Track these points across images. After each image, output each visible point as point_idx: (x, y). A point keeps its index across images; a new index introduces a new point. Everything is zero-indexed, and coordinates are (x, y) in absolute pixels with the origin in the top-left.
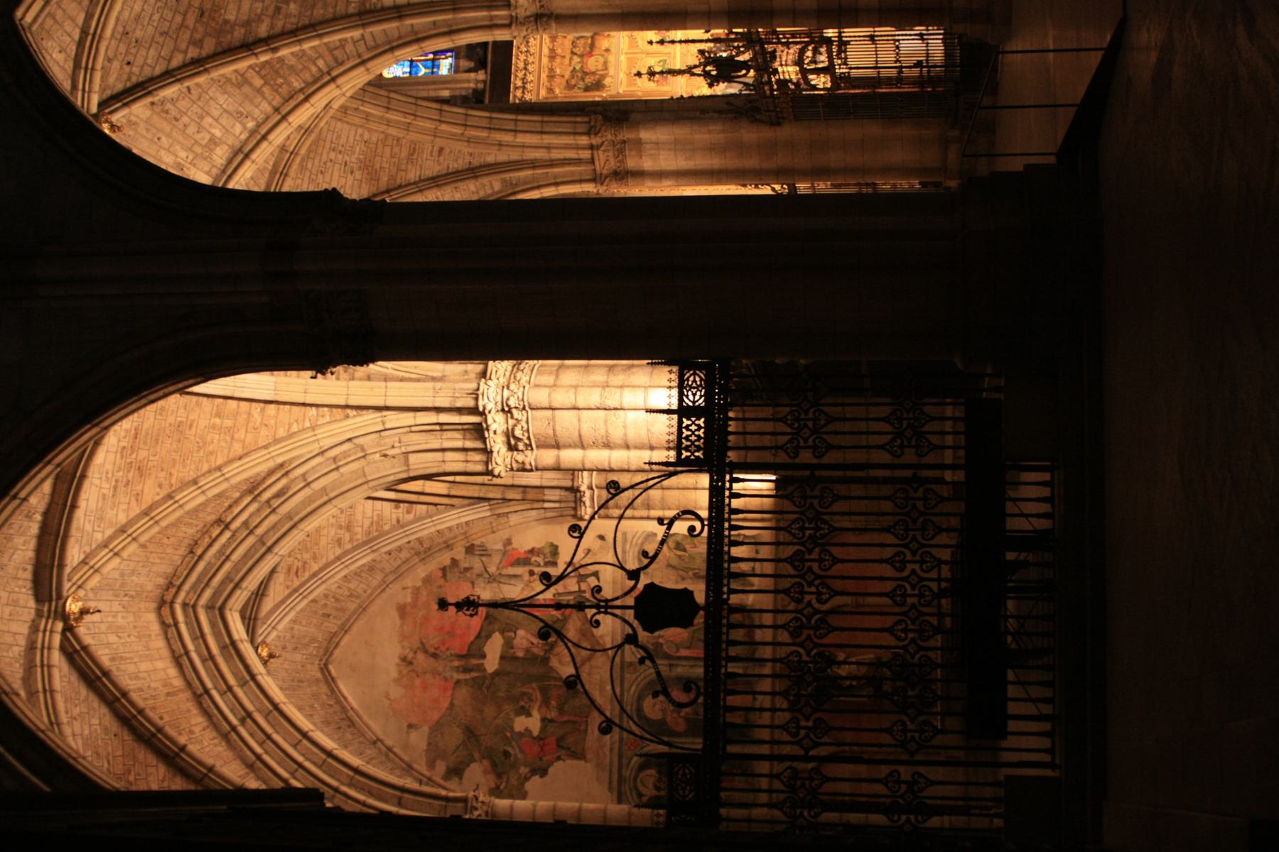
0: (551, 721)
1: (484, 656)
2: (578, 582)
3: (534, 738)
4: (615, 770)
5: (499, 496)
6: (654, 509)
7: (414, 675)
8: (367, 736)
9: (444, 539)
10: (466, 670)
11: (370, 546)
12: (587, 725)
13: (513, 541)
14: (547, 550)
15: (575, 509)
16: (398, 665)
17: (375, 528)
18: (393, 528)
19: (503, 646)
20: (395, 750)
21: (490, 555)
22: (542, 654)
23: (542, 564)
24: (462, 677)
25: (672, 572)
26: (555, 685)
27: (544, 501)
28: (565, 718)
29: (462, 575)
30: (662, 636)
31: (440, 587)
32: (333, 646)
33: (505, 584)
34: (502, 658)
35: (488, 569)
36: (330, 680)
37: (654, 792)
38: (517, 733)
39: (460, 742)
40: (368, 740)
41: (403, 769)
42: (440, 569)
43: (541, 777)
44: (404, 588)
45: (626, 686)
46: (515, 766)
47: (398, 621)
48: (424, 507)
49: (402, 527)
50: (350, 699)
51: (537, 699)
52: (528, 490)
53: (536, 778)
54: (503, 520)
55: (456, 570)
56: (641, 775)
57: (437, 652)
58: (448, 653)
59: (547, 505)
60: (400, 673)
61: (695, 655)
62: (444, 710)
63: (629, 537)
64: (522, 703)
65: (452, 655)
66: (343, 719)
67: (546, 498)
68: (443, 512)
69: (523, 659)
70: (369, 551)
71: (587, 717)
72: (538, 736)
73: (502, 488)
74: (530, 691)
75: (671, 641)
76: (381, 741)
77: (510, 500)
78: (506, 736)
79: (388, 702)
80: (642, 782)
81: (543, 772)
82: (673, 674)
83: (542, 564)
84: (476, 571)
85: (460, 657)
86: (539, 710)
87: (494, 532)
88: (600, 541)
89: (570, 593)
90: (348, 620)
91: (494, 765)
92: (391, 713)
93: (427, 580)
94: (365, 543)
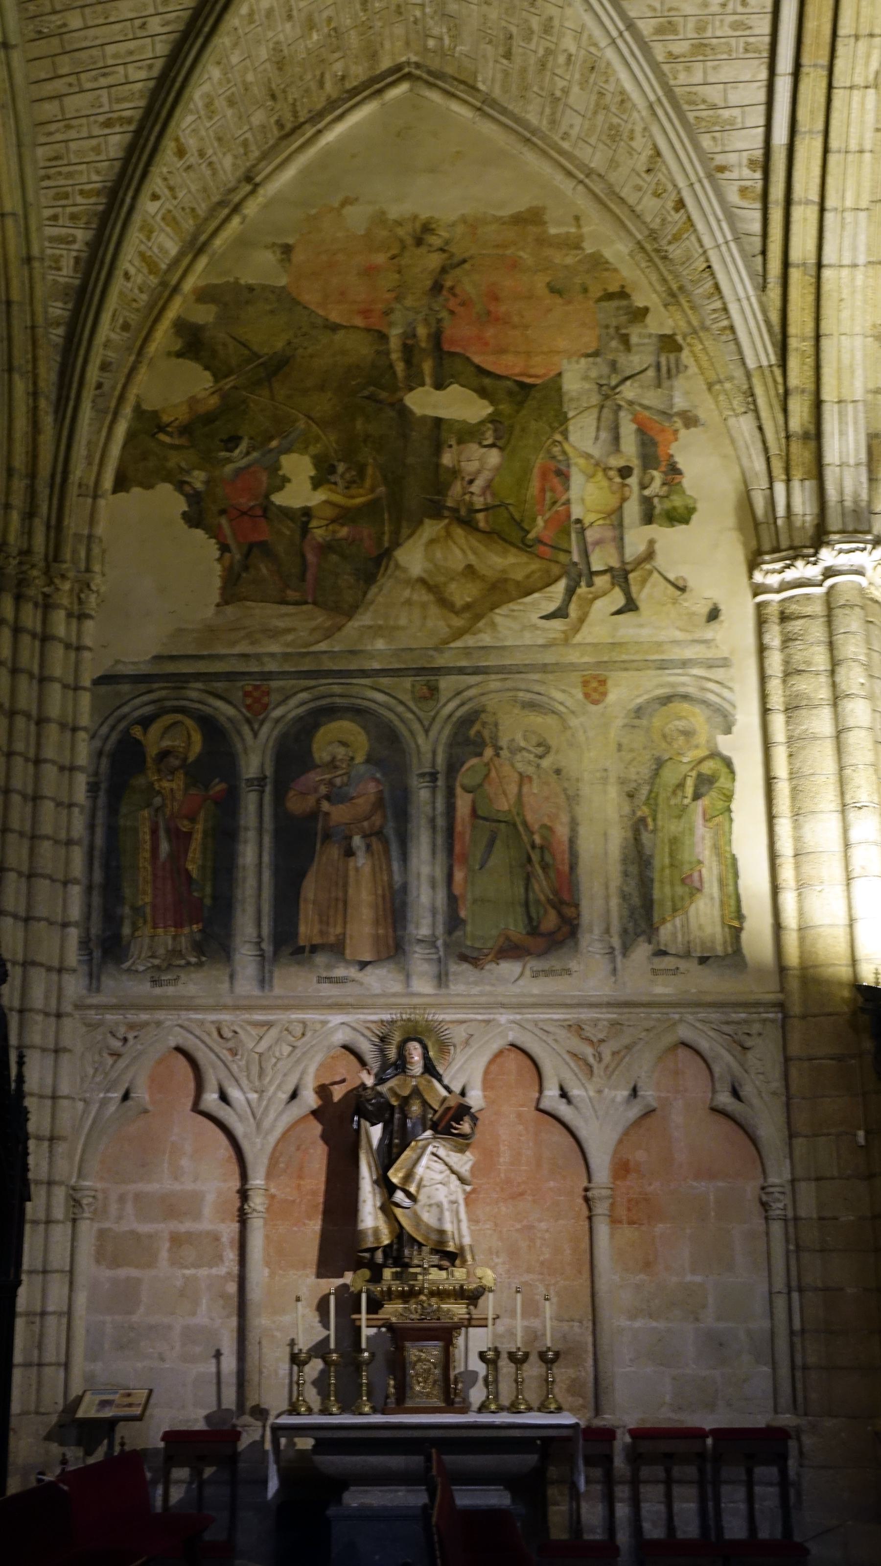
0: (305, 530)
1: (439, 386)
2: (610, 570)
3: (267, 496)
4: (202, 667)
5: (794, 381)
6: (788, 723)
7: (395, 251)
8: (263, 163)
9: (689, 287)
10: (409, 351)
11: (664, 100)
12: (296, 603)
13: (693, 430)
14: (677, 501)
15: (776, 550)
16: (415, 217)
17: (704, 114)
18: (705, 157)
19: (464, 422)
20: (236, 221)
21: (659, 385)
22: (450, 503)
23: (647, 492)
24: (394, 343)
25: (646, 771)
26: (383, 533)
27: (788, 481)
28: (311, 558)
29: (612, 331)
30: (498, 755)
31: (585, 290)
32: (447, 86)
33: (599, 419)
34: (438, 422)
35: (628, 383)
36: (377, 86)
37: (152, 751)
38: (277, 461)
39: (255, 348)
40: (254, 166)
41: (195, 237)
42: (623, 287)
43: (185, 515)
44: (577, 218)
45: (385, 681)
46: (208, 460)
47: (506, 212)
48: (756, 227)
49: (710, 177)
50: (340, 128)
51: (352, 497)
52: (812, 444)
53: (182, 505)
54: (738, 402)
55: (623, 319)
56: (189, 722)
57: (445, 292)
58: (444, 314)
59: (780, 488)
60: (399, 223)
61: (459, 828)
62: (321, 312)
63: (719, 674)
64: (341, 468)
65: (439, 321)
66: (295, 114)
67: (796, 484)
68: (748, 267)
69: (438, 465)
70: (652, 98)
71: (315, 603)
72: (272, 503)
73: (810, 386)
74: (368, 483)
75: (487, 776)
76: (253, 192)
77: (785, 410)
78: (271, 438)
79: (336, 205)
80: (175, 724)
81: (194, 519)
82: (414, 782)
83: (647, 492)
84: (623, 360)
85: (437, 338)
86: (326, 502)
87: (710, 386)
88: (704, 609)
89: (585, 554)
90: (504, 111)
91: (209, 418)
92: (313, 211)
93: (597, 263)
94: (669, 92)
